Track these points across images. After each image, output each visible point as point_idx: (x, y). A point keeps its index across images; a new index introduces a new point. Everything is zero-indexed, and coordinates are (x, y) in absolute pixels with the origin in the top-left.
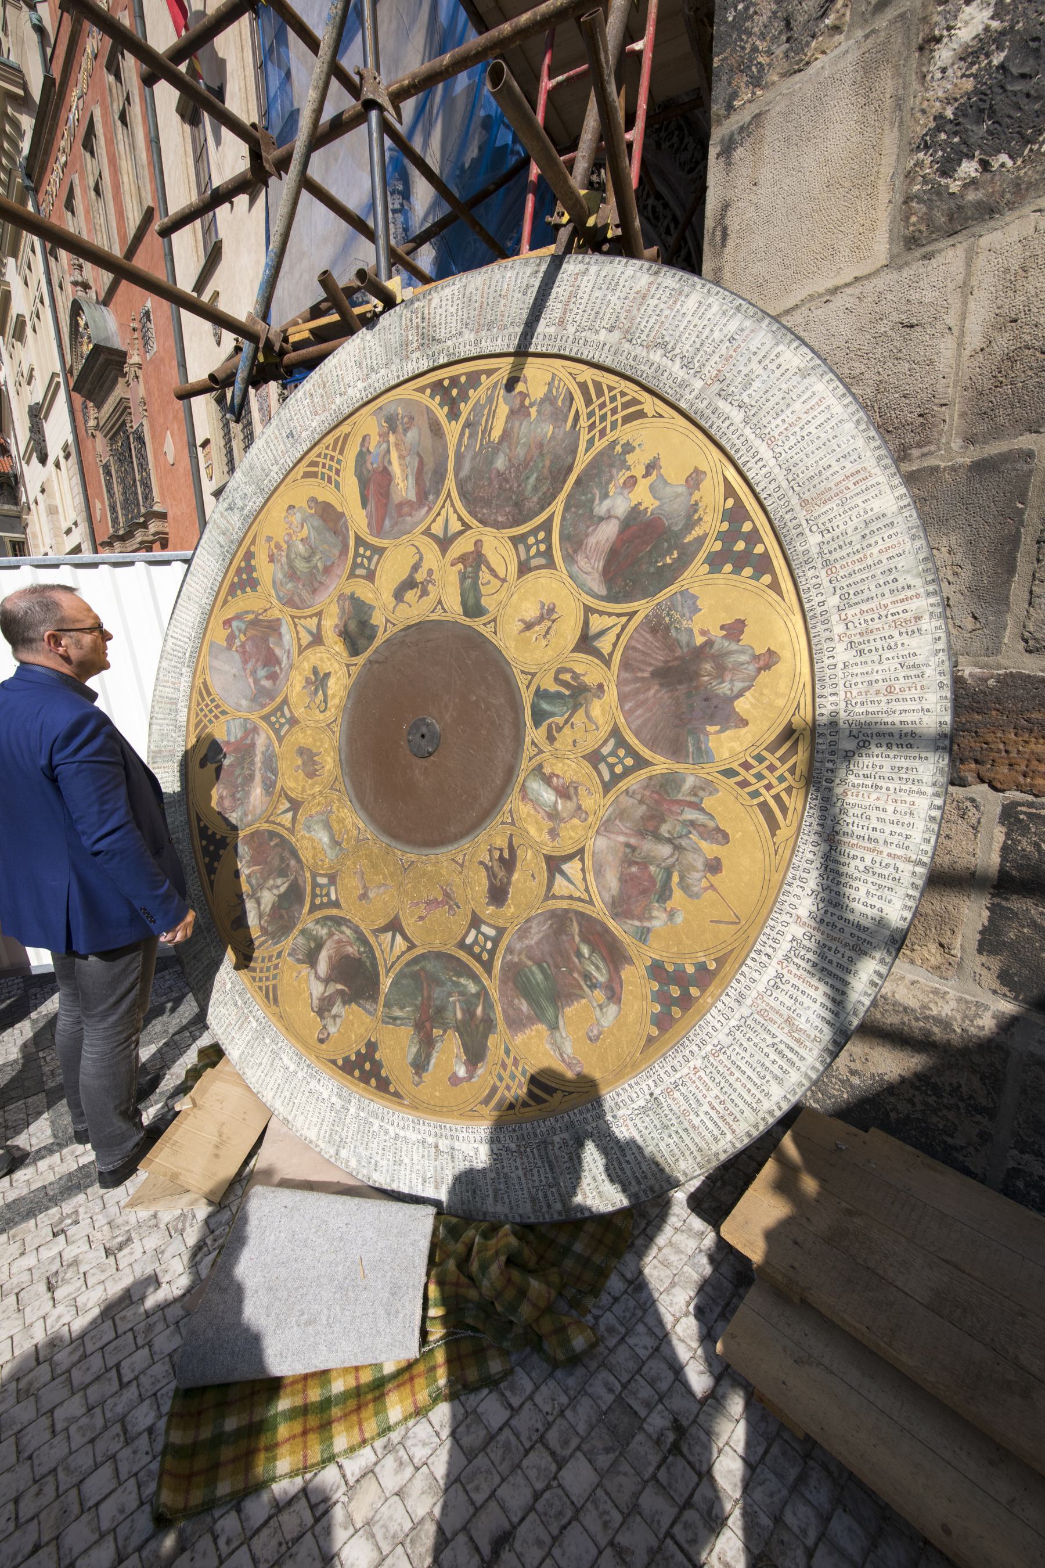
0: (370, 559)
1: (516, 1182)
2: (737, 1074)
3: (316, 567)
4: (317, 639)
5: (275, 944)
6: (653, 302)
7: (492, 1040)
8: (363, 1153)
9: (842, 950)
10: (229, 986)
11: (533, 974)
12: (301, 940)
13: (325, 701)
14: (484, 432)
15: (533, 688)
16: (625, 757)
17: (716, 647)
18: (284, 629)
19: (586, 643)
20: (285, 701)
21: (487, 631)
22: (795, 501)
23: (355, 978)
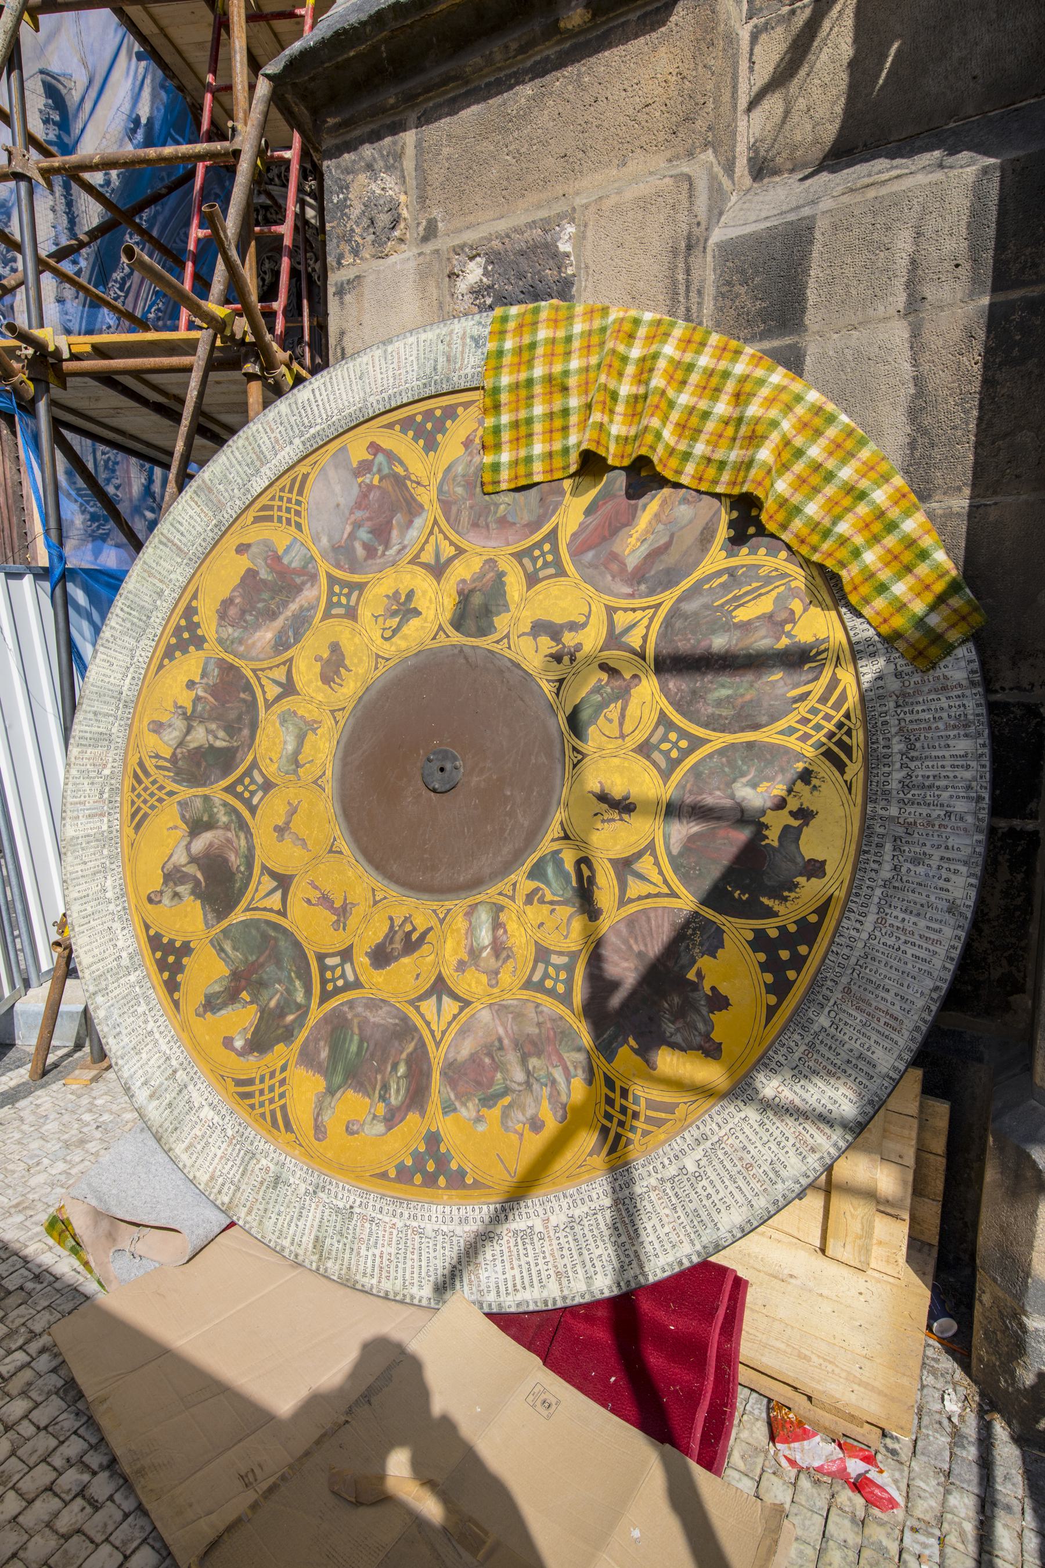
0: (546, 564)
1: (211, 1155)
2: (416, 1257)
5: (174, 781)
6: (944, 703)
7: (280, 1048)
8: (116, 1016)
9: (550, 1266)
11: (351, 1040)
12: (198, 803)
13: (395, 631)
14: (736, 598)
15: (556, 846)
16: (562, 981)
17: (695, 995)
18: (418, 522)
20: (361, 587)
22: (844, 980)
23: (219, 883)
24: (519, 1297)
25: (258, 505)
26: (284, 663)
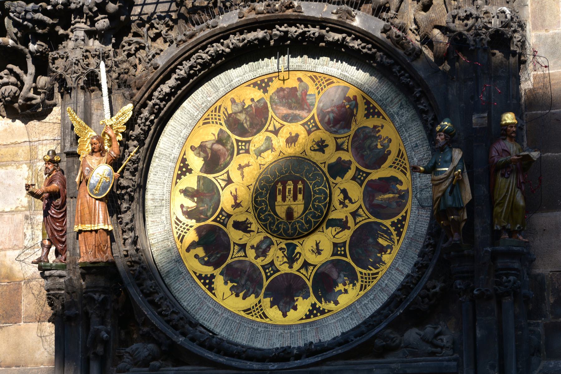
3: (365, 151)
4: (339, 148)
7: (194, 221)
10: (209, 99)
12: (226, 135)
13: (315, 150)
14: (382, 235)
15: (298, 244)
18: (346, 130)
19: (306, 265)
21: (321, 229)
22: (319, 326)
24: (204, 322)
25: (315, 74)
26: (281, 124)
